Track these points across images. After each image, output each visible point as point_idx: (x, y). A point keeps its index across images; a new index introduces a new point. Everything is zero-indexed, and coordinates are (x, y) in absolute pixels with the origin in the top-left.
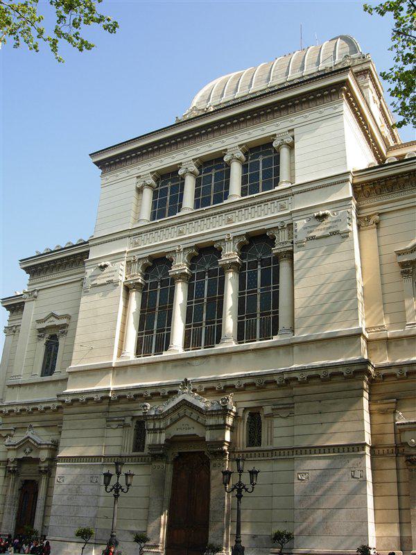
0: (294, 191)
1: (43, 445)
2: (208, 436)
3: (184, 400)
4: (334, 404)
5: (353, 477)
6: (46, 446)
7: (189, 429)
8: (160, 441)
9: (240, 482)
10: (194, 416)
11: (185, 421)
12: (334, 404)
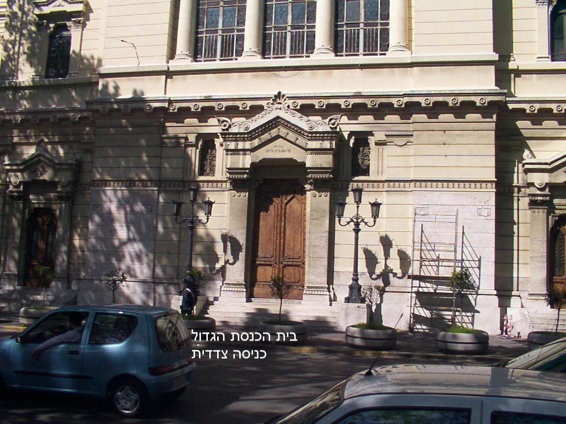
1: (64, 164)
2: (310, 161)
3: (278, 117)
4: (461, 135)
5: (480, 215)
6: (67, 167)
8: (244, 164)
9: (358, 215)
10: (292, 136)
12: (461, 135)
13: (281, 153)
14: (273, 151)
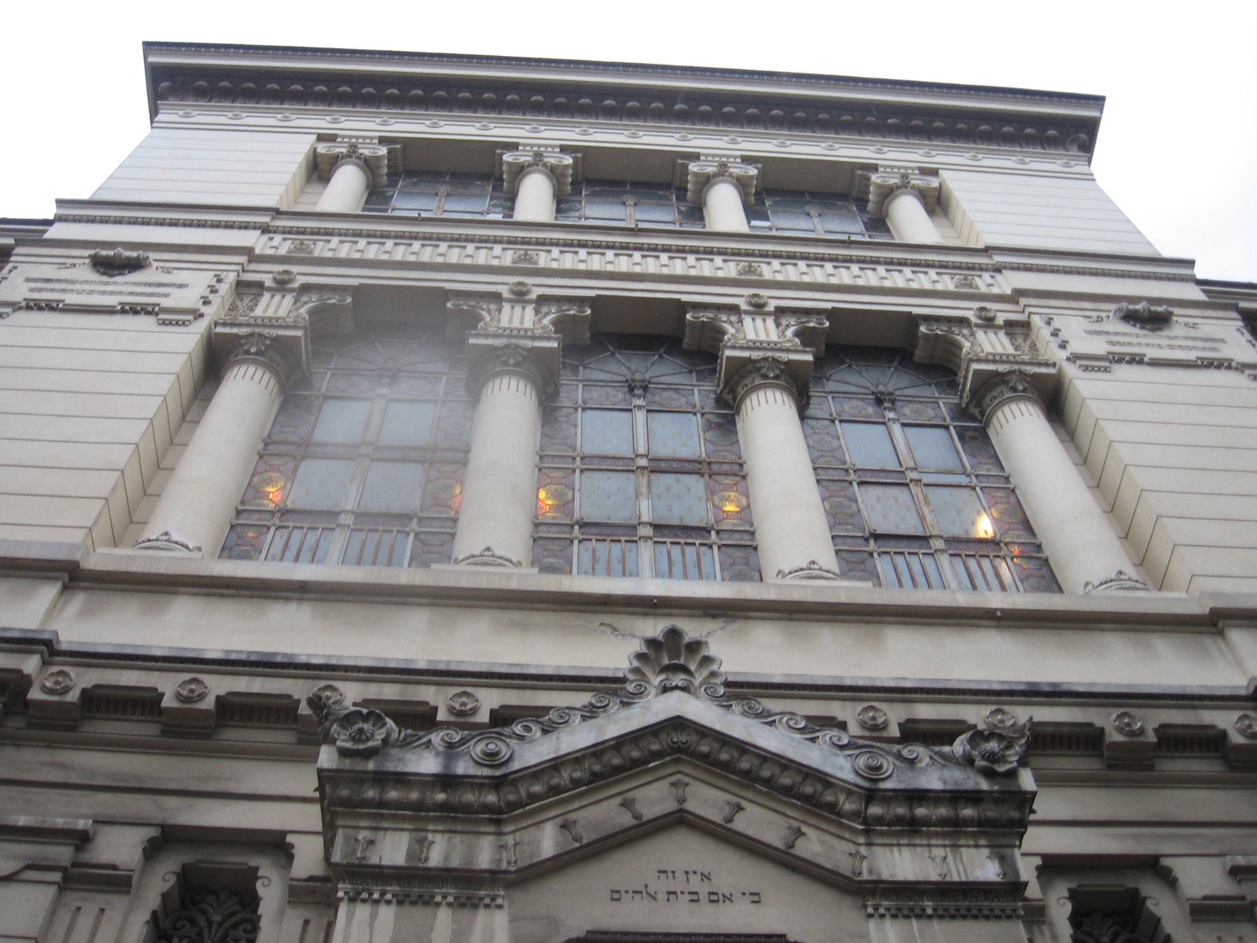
0: (998, 259)
3: (678, 723)
7: (715, 898)
10: (761, 822)
11: (683, 852)
13: (706, 909)
14: (653, 897)
